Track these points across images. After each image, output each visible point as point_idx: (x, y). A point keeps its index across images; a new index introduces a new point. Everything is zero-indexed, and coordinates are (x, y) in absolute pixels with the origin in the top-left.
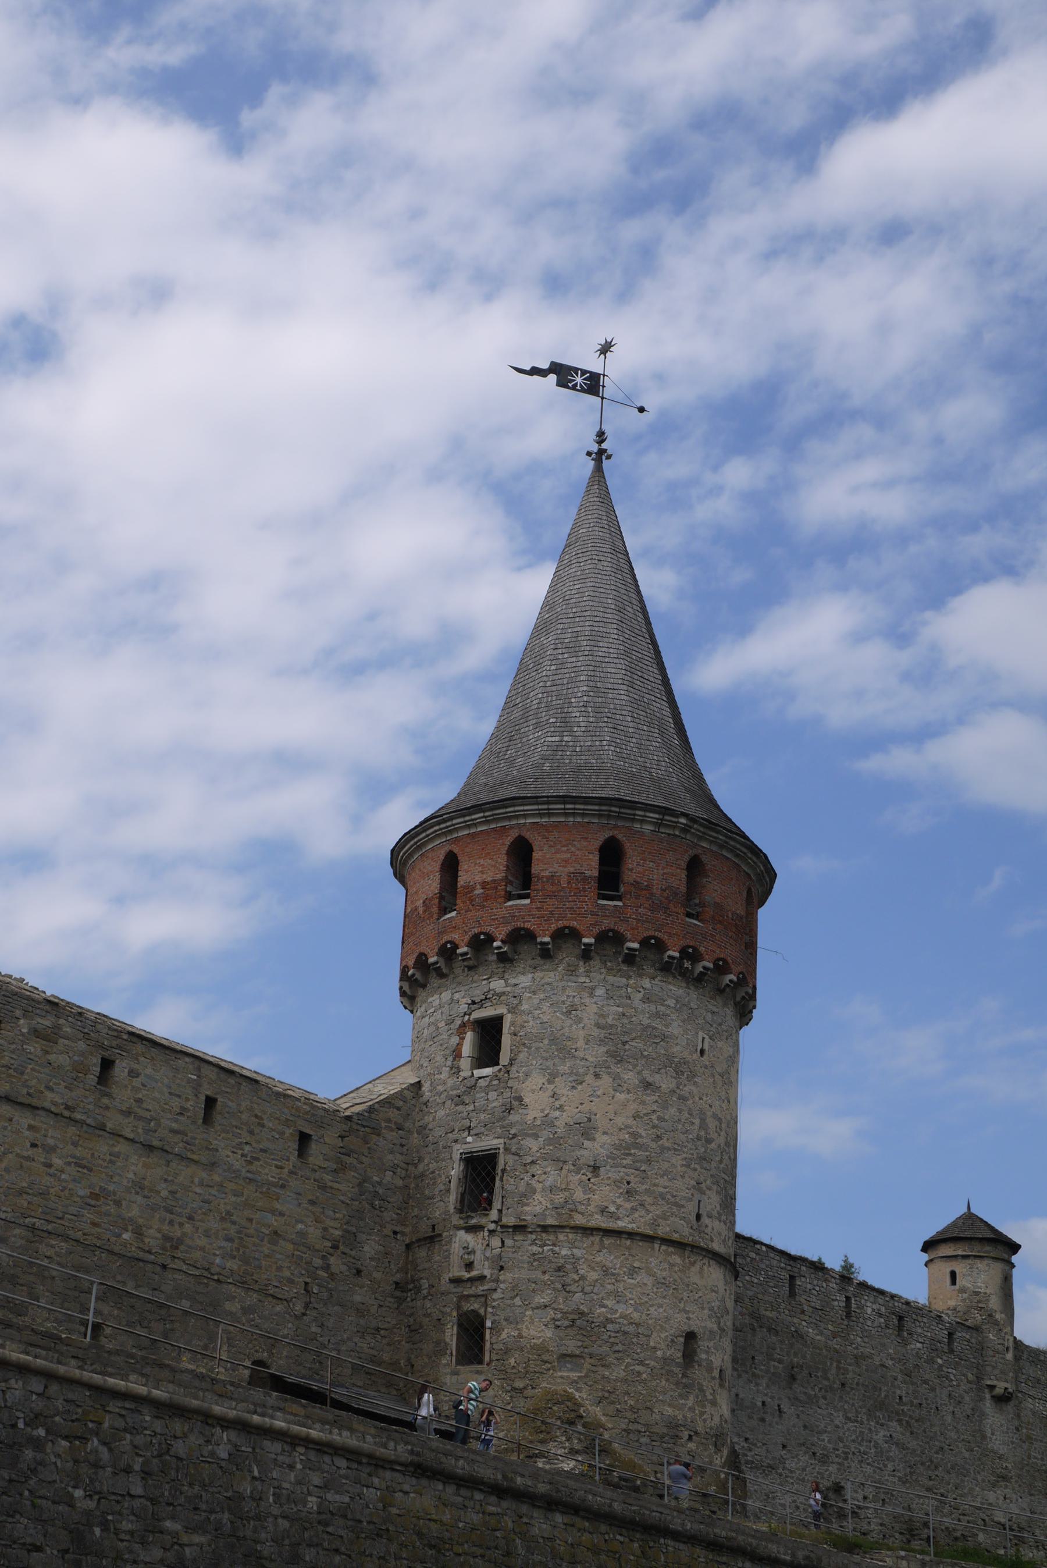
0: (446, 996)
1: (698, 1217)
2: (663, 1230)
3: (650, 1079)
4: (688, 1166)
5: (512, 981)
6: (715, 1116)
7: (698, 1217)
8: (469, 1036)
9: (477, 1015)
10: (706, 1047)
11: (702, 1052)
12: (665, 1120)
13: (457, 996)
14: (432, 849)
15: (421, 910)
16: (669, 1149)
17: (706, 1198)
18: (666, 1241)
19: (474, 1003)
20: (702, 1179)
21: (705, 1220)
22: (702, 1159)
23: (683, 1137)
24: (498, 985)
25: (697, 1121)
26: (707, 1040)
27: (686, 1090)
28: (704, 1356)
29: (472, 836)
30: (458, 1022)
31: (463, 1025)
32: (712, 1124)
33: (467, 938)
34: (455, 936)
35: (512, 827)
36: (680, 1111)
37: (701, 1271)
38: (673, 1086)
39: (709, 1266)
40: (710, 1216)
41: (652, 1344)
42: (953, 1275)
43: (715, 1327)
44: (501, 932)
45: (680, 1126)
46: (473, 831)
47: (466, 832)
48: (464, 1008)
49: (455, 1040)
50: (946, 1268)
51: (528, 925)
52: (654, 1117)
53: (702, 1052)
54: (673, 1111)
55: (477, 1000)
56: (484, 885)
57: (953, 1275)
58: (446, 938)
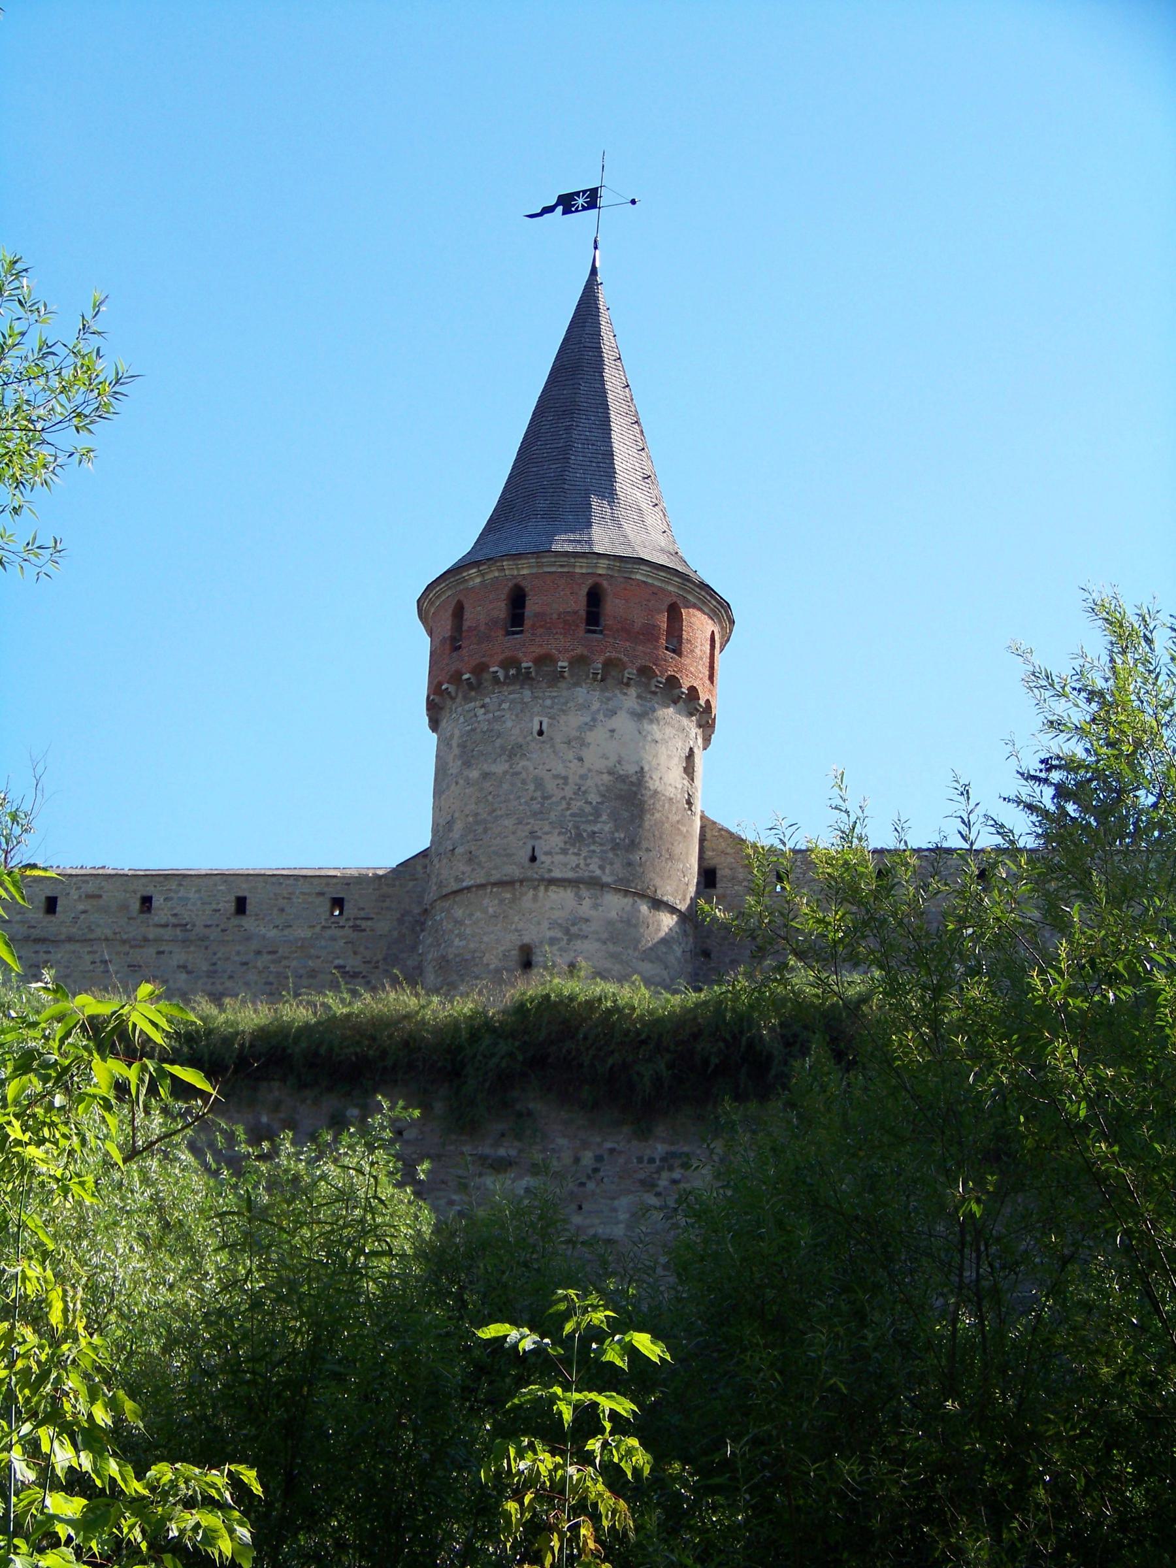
1: (533, 859)
2: (492, 880)
3: (487, 770)
4: (520, 823)
6: (556, 777)
7: (533, 859)
10: (544, 727)
11: (541, 733)
12: (498, 796)
16: (502, 816)
17: (542, 842)
18: (494, 884)
20: (536, 828)
21: (541, 857)
22: (535, 814)
23: (516, 803)
25: (532, 787)
26: (546, 721)
27: (518, 768)
28: (541, 959)
32: (551, 786)
36: (512, 784)
37: (535, 899)
38: (507, 766)
39: (546, 890)
40: (546, 853)
41: (485, 961)
43: (560, 935)
45: (512, 797)
52: (490, 798)
53: (541, 733)
54: (506, 786)
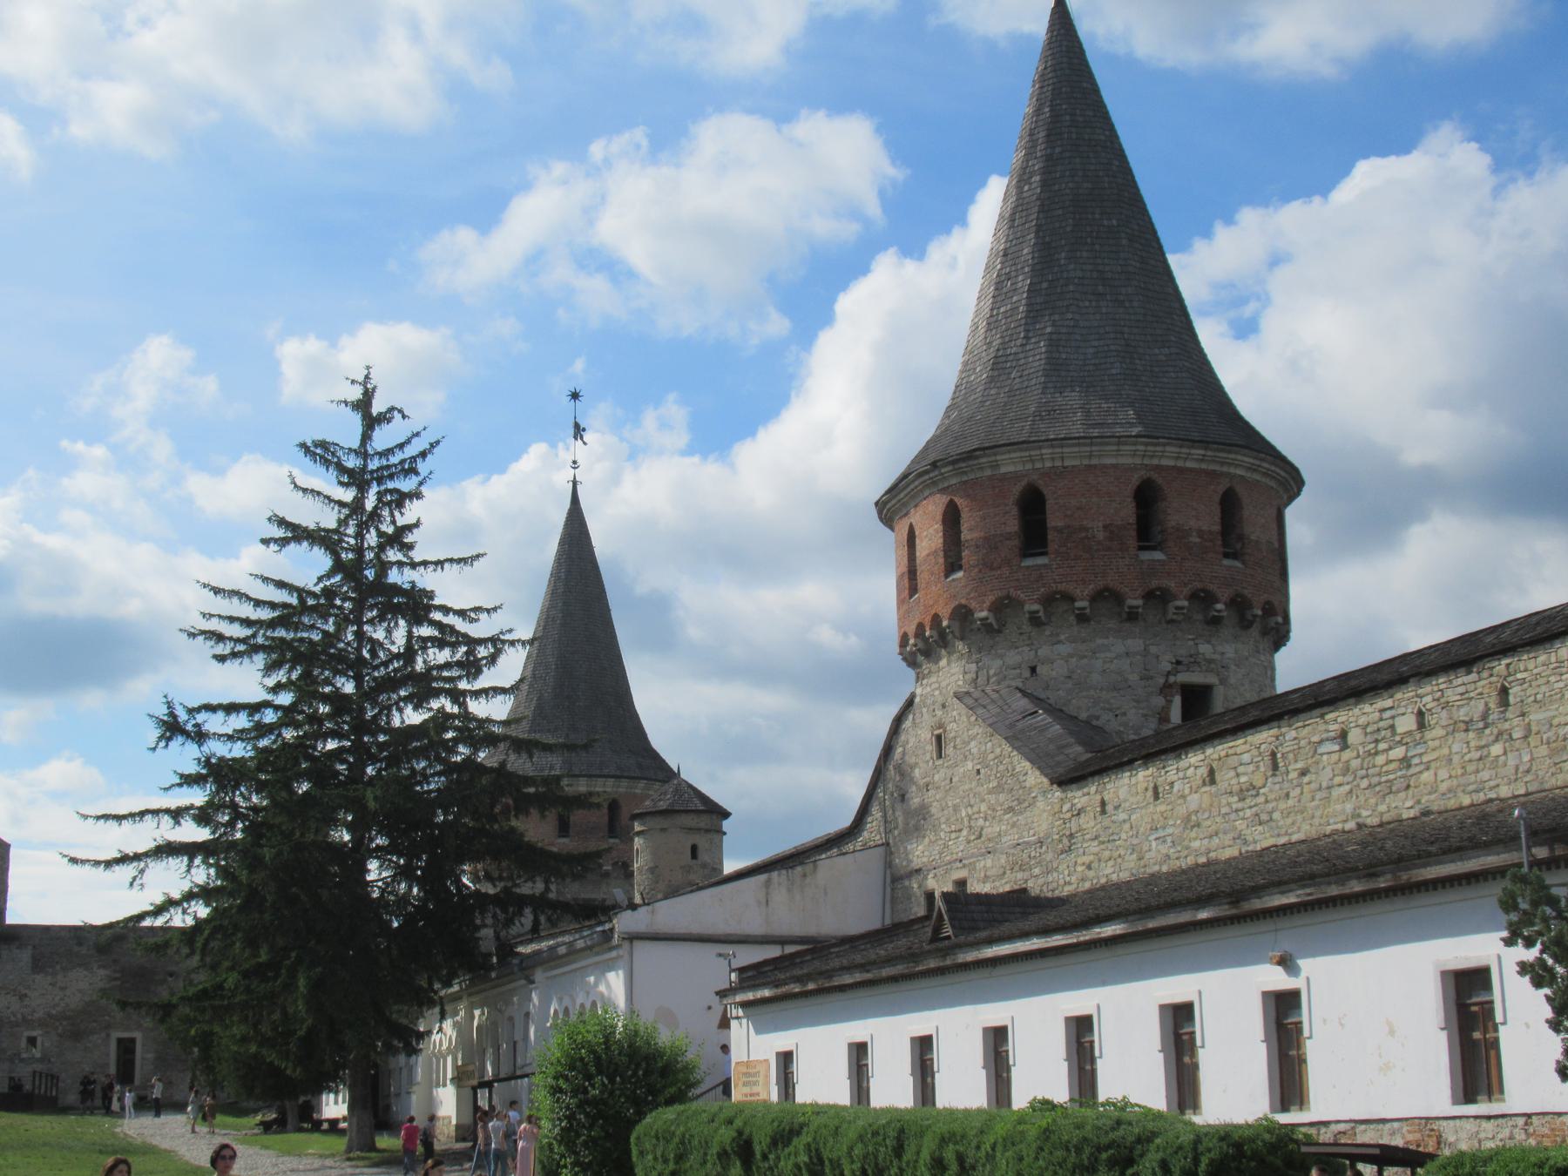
0: (1135, 644)
5: (1220, 649)
8: (1177, 701)
9: (1183, 678)
13: (1153, 649)
14: (1115, 466)
15: (1101, 535)
19: (1178, 663)
24: (1205, 649)
29: (1181, 470)
30: (1162, 681)
31: (1166, 689)
33: (1186, 591)
34: (1171, 584)
35: (1222, 474)
42: (694, 849)
44: (1224, 594)
46: (1180, 464)
47: (1171, 463)
48: (1166, 666)
49: (1159, 701)
50: (689, 841)
51: (1246, 592)
55: (1185, 661)
56: (1200, 533)
57: (694, 849)
58: (1154, 583)
